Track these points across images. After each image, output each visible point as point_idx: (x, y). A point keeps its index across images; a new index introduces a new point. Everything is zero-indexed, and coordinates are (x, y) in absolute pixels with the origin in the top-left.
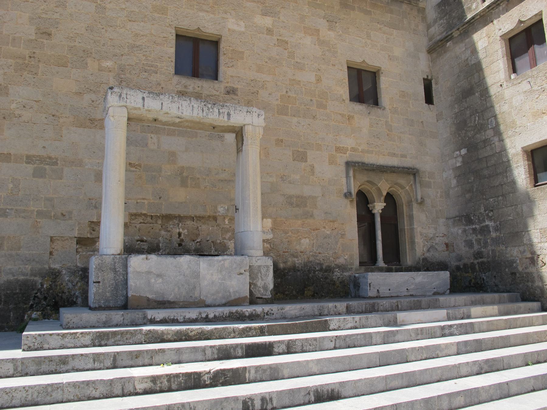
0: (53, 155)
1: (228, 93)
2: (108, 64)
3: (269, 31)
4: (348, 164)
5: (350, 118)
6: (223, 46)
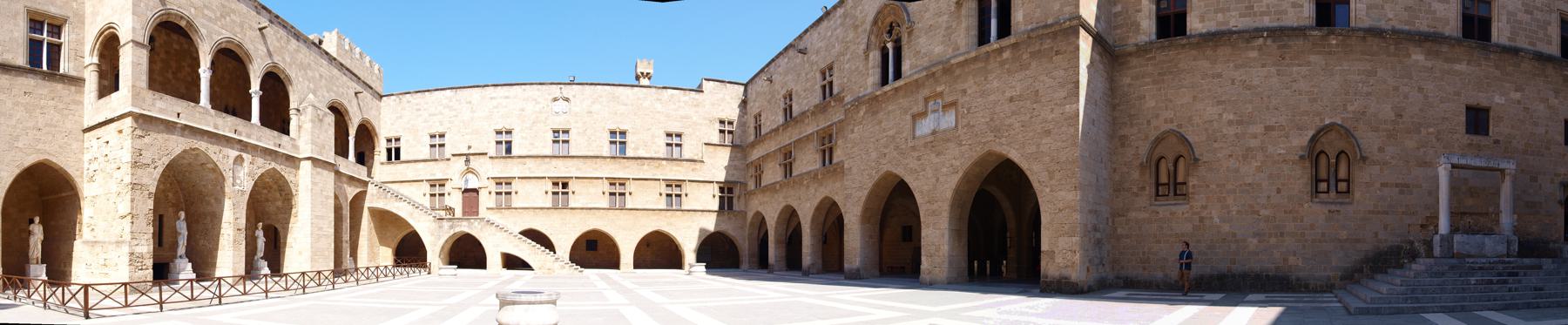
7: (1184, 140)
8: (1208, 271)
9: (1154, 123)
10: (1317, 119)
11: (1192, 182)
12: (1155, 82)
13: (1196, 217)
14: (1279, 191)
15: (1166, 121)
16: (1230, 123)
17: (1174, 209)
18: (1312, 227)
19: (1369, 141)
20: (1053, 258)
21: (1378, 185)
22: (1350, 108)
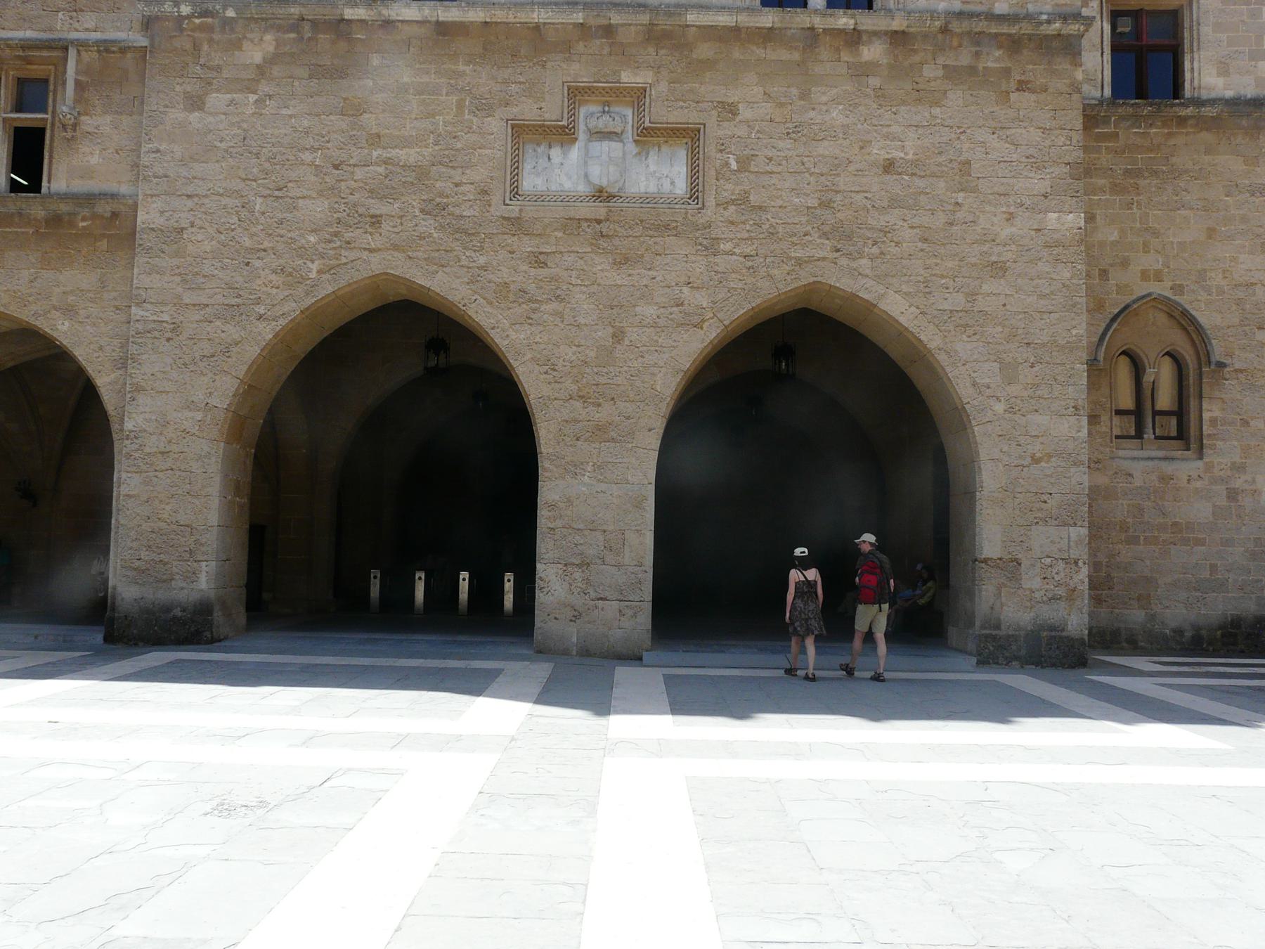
7: (1186, 321)
9: (1116, 276)
11: (1211, 411)
12: (1116, 189)
13: (1221, 489)
15: (1145, 275)
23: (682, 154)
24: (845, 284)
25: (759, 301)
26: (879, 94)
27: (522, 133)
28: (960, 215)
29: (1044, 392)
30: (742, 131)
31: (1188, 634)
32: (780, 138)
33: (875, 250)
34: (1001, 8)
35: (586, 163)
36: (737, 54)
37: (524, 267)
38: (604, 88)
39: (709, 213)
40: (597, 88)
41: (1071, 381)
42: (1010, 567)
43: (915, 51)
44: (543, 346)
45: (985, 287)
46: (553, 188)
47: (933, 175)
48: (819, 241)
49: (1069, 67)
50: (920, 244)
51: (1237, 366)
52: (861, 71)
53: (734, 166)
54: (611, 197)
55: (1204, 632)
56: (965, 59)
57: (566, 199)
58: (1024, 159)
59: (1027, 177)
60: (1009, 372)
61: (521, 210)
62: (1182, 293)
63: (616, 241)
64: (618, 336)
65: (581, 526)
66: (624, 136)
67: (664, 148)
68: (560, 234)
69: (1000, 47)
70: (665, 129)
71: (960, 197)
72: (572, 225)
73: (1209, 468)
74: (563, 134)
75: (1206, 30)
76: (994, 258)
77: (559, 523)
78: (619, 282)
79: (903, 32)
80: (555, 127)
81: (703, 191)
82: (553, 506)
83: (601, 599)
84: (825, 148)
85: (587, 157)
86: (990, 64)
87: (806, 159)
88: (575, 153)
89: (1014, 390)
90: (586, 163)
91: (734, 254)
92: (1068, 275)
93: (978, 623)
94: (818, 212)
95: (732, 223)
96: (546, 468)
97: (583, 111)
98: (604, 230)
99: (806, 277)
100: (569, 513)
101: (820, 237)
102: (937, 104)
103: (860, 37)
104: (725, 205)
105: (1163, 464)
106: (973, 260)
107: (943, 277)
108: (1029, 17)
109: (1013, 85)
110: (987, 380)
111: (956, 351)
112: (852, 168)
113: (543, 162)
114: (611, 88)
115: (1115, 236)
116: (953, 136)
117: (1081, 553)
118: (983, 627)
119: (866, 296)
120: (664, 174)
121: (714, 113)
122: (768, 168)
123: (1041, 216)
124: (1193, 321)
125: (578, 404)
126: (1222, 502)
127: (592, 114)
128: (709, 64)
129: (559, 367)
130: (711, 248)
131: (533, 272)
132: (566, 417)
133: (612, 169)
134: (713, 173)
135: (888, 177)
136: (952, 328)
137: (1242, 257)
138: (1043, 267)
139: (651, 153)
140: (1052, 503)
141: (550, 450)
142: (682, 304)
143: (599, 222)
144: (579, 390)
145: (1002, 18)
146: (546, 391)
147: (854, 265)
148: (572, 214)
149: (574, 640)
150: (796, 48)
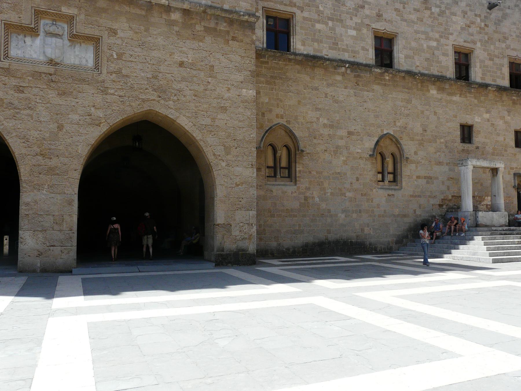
0: (431, 176)
1: (476, 148)
2: (442, 140)
3: (488, 120)
4: (515, 174)
5: (515, 155)
6: (474, 129)
8: (310, 239)
9: (268, 116)
10: (379, 130)
12: (268, 83)
13: (302, 196)
14: (358, 179)
15: (277, 116)
16: (325, 126)
17: (285, 188)
18: (378, 206)
19: (409, 147)
20: (229, 231)
21: (415, 177)
22: (398, 124)
23: (91, 48)
24: (163, 111)
25: (126, 116)
26: (178, 34)
27: (10, 28)
28: (209, 87)
29: (240, 158)
30: (119, 42)
31: (291, 250)
32: (136, 47)
33: (175, 98)
34: (226, 7)
35: (44, 46)
36: (117, 8)
37: (12, 92)
38: (53, 13)
39: (103, 77)
40: (49, 12)
41: (250, 155)
42: (228, 227)
43: (193, 19)
44: (21, 130)
45: (218, 116)
46: (27, 56)
47: (199, 70)
48: (152, 92)
49: (250, 33)
50: (193, 97)
51: (308, 152)
52: (171, 23)
53: (115, 57)
54: (56, 64)
55: (296, 249)
56: (212, 25)
57: (33, 62)
58: (234, 67)
59: (235, 74)
60: (227, 150)
61: (9, 65)
62: (290, 124)
63: (59, 85)
64: (60, 127)
65: (42, 213)
66: (63, 37)
67: (83, 45)
68: (31, 78)
69: (226, 22)
70: (84, 36)
71: (210, 79)
72: (37, 75)
73: (298, 188)
74: (33, 32)
75: (298, 28)
76: (222, 105)
77: (31, 212)
78: (61, 103)
79: (188, 10)
80: (28, 27)
81: (101, 66)
82: (27, 204)
83: (52, 246)
84: (155, 54)
85: (44, 44)
86: (222, 28)
87: (147, 57)
88: (38, 41)
89: (229, 157)
90: (44, 46)
91: (115, 95)
92: (250, 114)
93: (215, 250)
94: (152, 80)
95: (114, 81)
96: (24, 186)
97: (42, 22)
98: (53, 79)
99: (146, 107)
100: (36, 207)
101: (152, 91)
102: (201, 41)
103: (170, 9)
104: (111, 73)
105: (283, 187)
106: (214, 105)
107: (202, 111)
108: (236, 12)
109: (230, 38)
110: (219, 153)
111: (207, 141)
112: (166, 63)
113: (21, 43)
114: (57, 14)
115: (267, 100)
116: (207, 55)
117: (254, 221)
118: (217, 251)
119: (171, 117)
120: (82, 56)
121: (106, 32)
122: (130, 59)
123: (240, 90)
124: (293, 134)
125: (40, 158)
126: (303, 201)
127: (47, 24)
128: (104, 10)
129: (31, 140)
130: (104, 91)
131: (16, 95)
132: (34, 164)
133: (57, 51)
134: (106, 58)
135: (181, 69)
136: (205, 132)
137: (309, 112)
138: (240, 110)
139: (77, 46)
140: (243, 202)
141: (27, 179)
142: (91, 115)
143: (51, 75)
144: (41, 151)
145: (226, 11)
146: (24, 151)
147: (167, 103)
148: (37, 70)
149: (39, 265)
150: (143, 9)
